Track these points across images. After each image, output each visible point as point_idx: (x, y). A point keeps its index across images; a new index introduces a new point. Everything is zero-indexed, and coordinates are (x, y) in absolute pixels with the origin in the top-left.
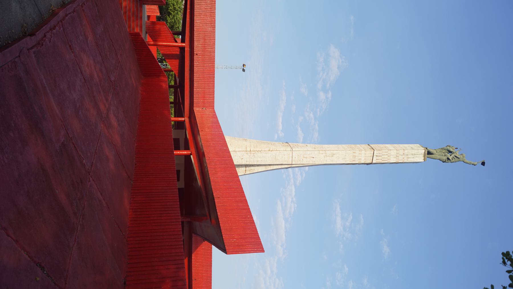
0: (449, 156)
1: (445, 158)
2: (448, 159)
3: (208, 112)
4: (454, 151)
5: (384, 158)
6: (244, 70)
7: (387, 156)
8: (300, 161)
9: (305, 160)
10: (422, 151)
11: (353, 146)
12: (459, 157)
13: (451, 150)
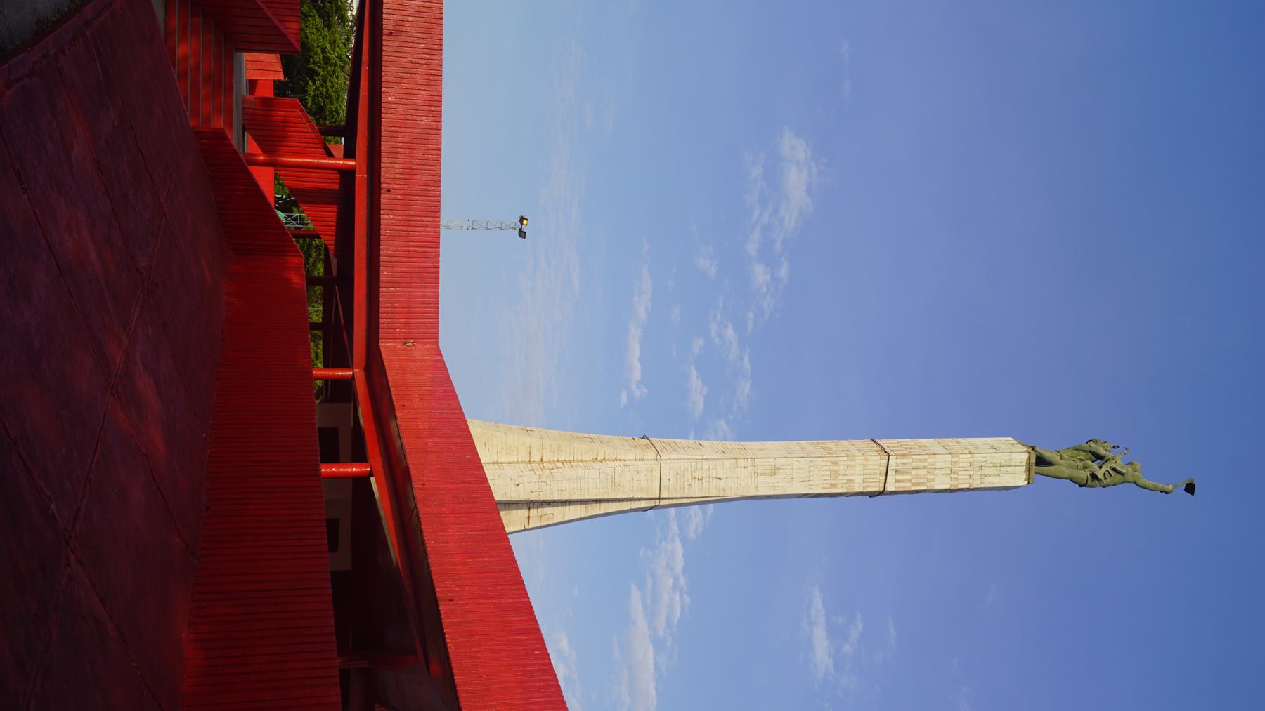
0: (1095, 469)
1: (1084, 475)
2: (1094, 477)
3: (419, 352)
4: (1110, 455)
5: (918, 477)
6: (522, 234)
7: (925, 472)
8: (682, 488)
9: (696, 484)
10: (1021, 456)
11: (829, 444)
12: (1123, 471)
13: (1102, 452)
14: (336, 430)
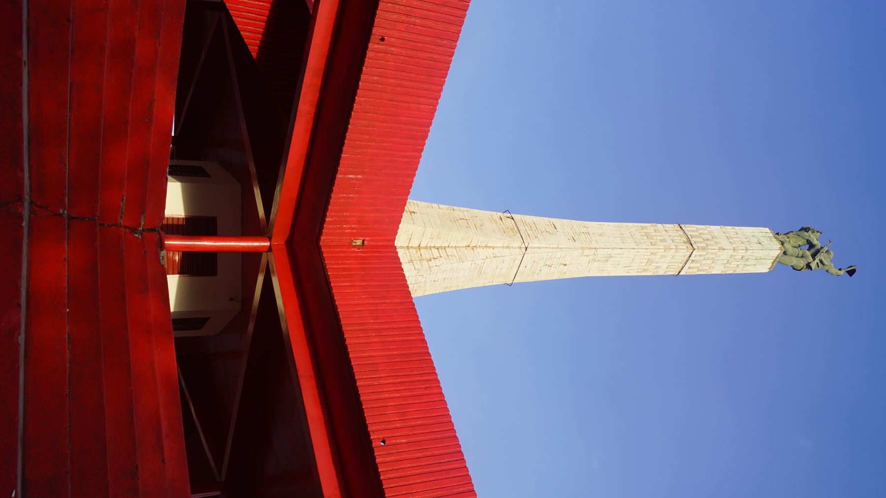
10: (774, 250)
11: (650, 227)
14: (215, 219)
